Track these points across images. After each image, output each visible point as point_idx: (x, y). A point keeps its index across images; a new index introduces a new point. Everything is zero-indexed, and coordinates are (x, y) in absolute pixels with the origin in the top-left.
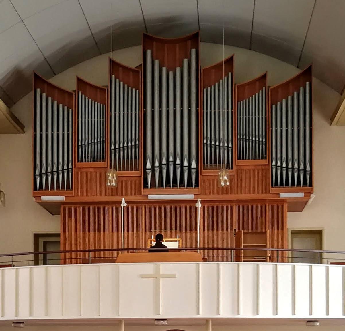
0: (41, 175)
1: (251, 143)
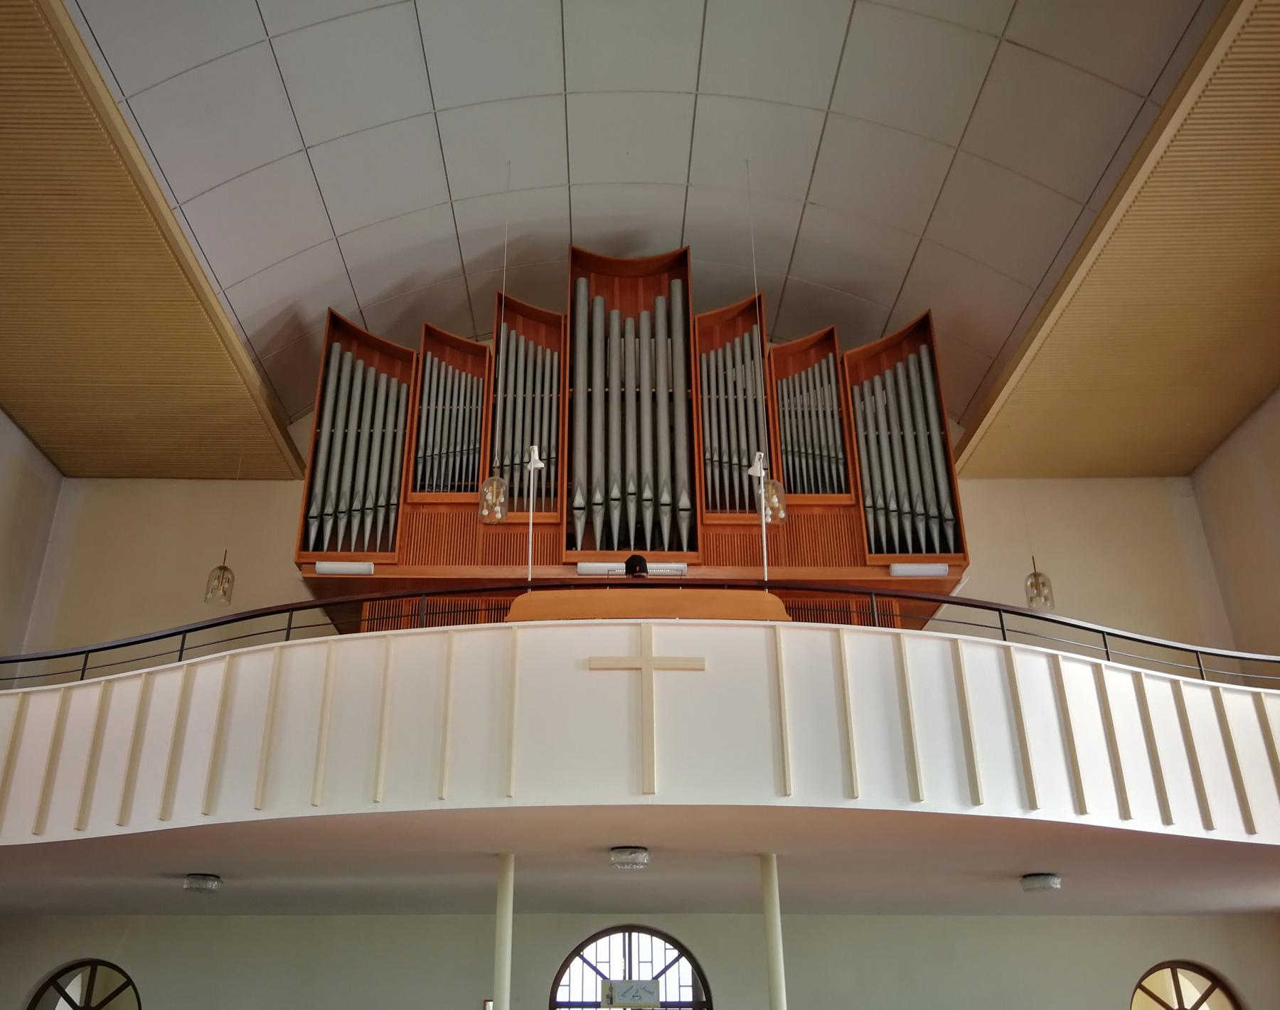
1: (811, 461)
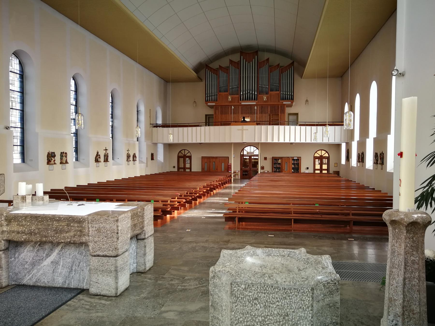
0: (208, 97)
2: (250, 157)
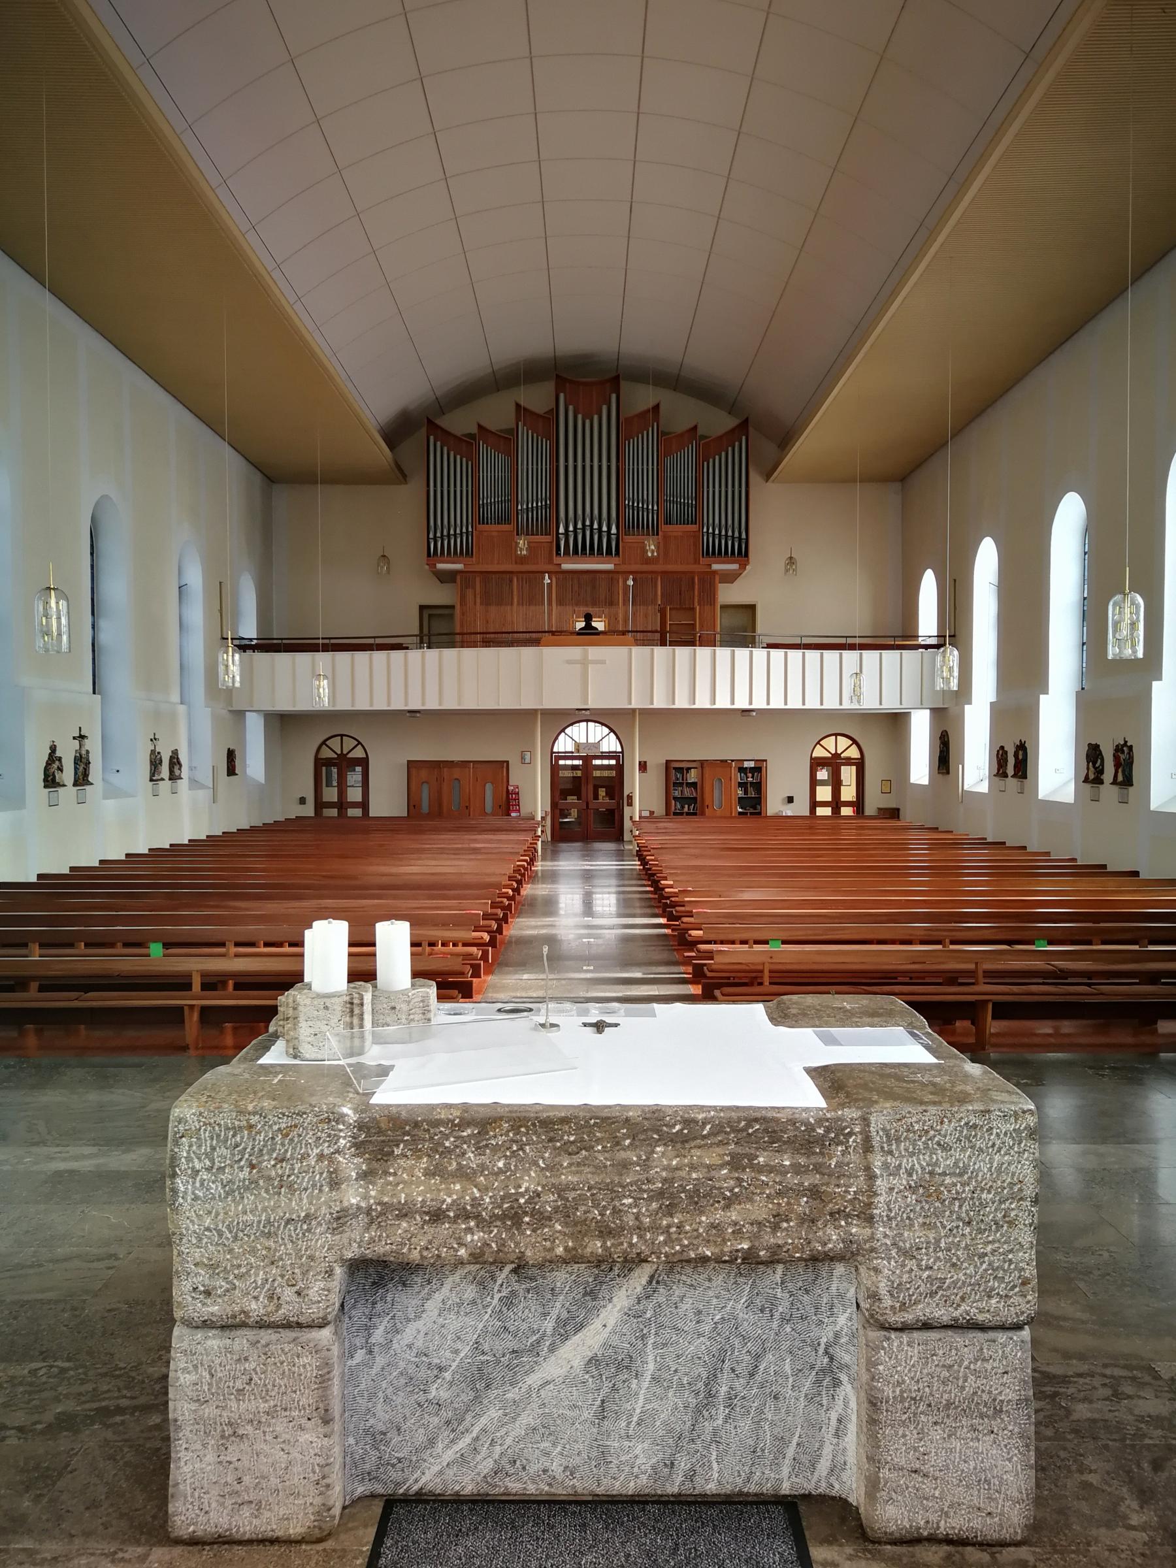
2: (587, 759)
